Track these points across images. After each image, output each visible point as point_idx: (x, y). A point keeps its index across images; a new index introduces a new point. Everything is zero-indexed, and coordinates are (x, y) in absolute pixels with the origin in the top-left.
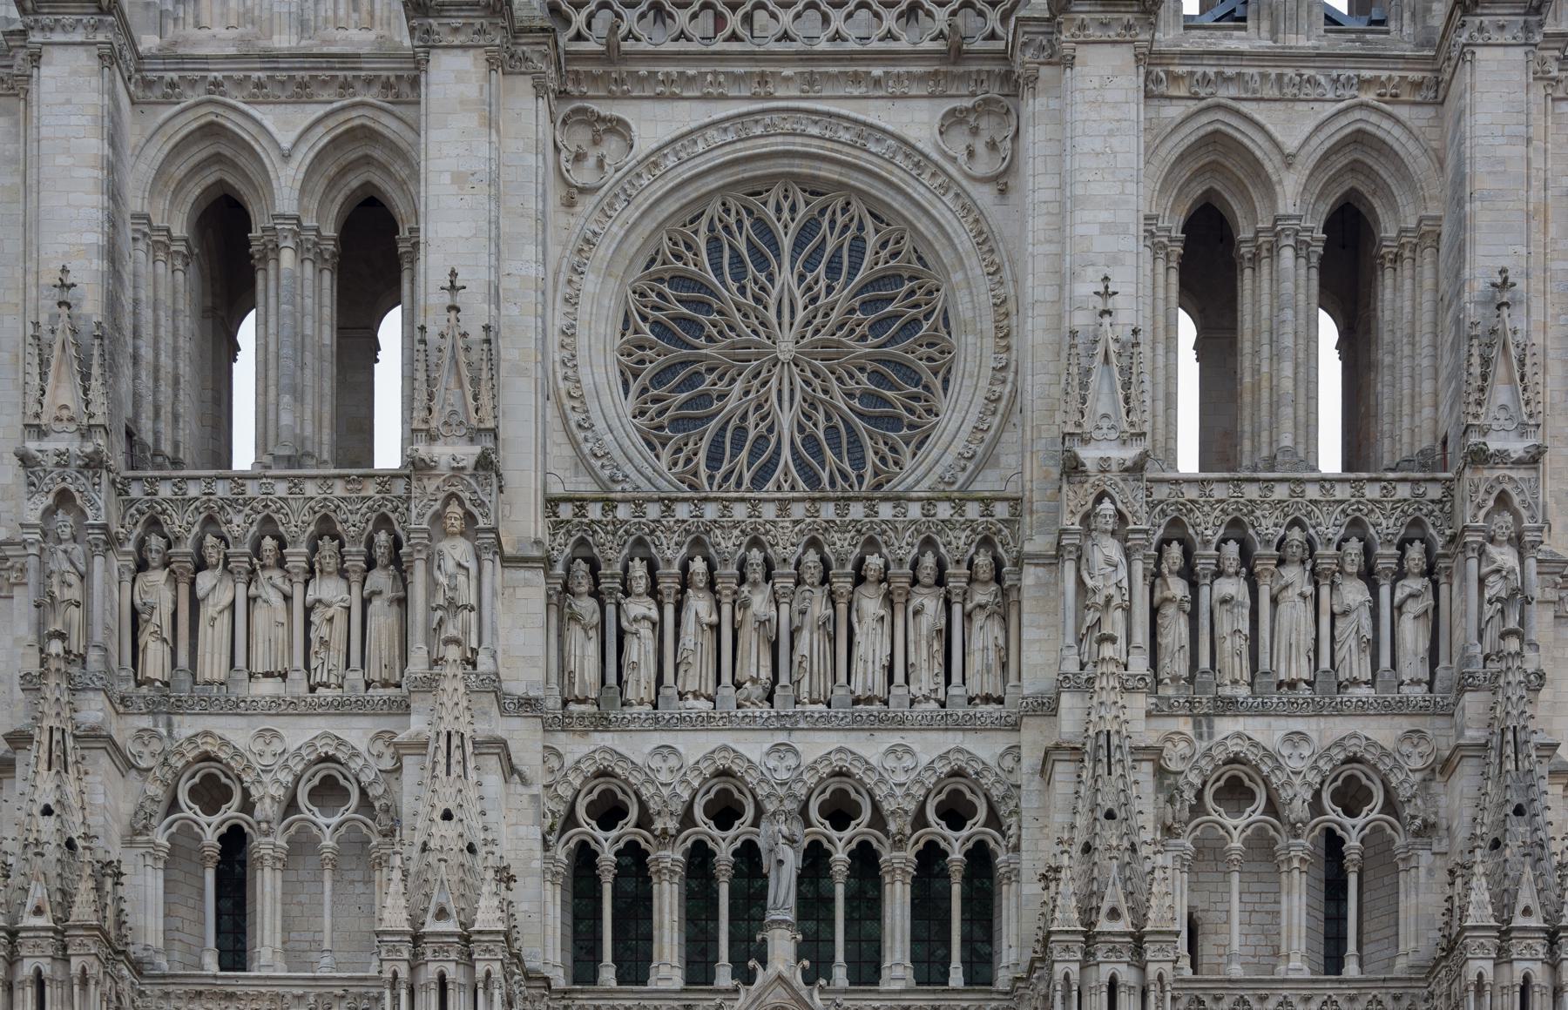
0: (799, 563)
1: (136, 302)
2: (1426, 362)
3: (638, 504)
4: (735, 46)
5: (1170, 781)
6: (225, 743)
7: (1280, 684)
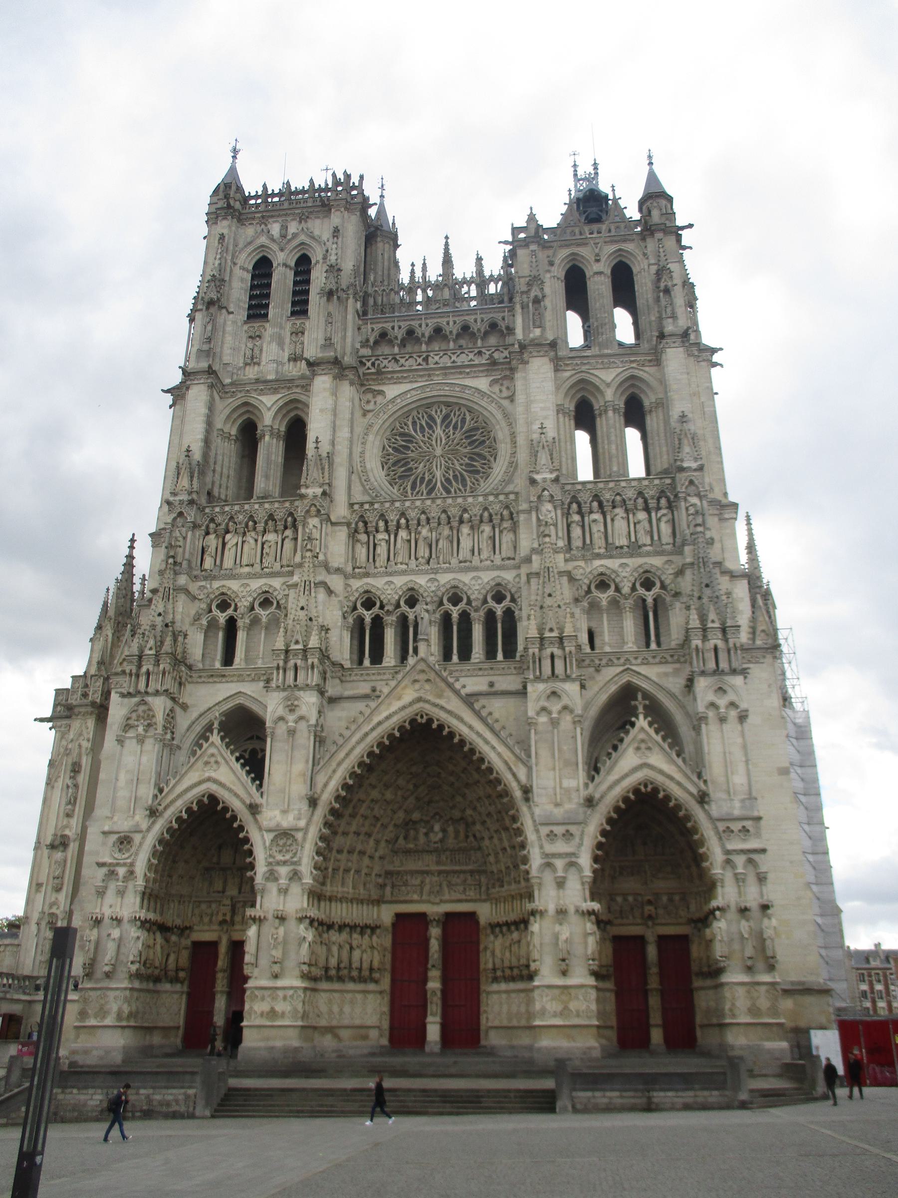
0: (439, 518)
1: (216, 454)
2: (663, 442)
3: (382, 503)
4: (420, 367)
5: (576, 583)
6: (230, 589)
7: (617, 548)
